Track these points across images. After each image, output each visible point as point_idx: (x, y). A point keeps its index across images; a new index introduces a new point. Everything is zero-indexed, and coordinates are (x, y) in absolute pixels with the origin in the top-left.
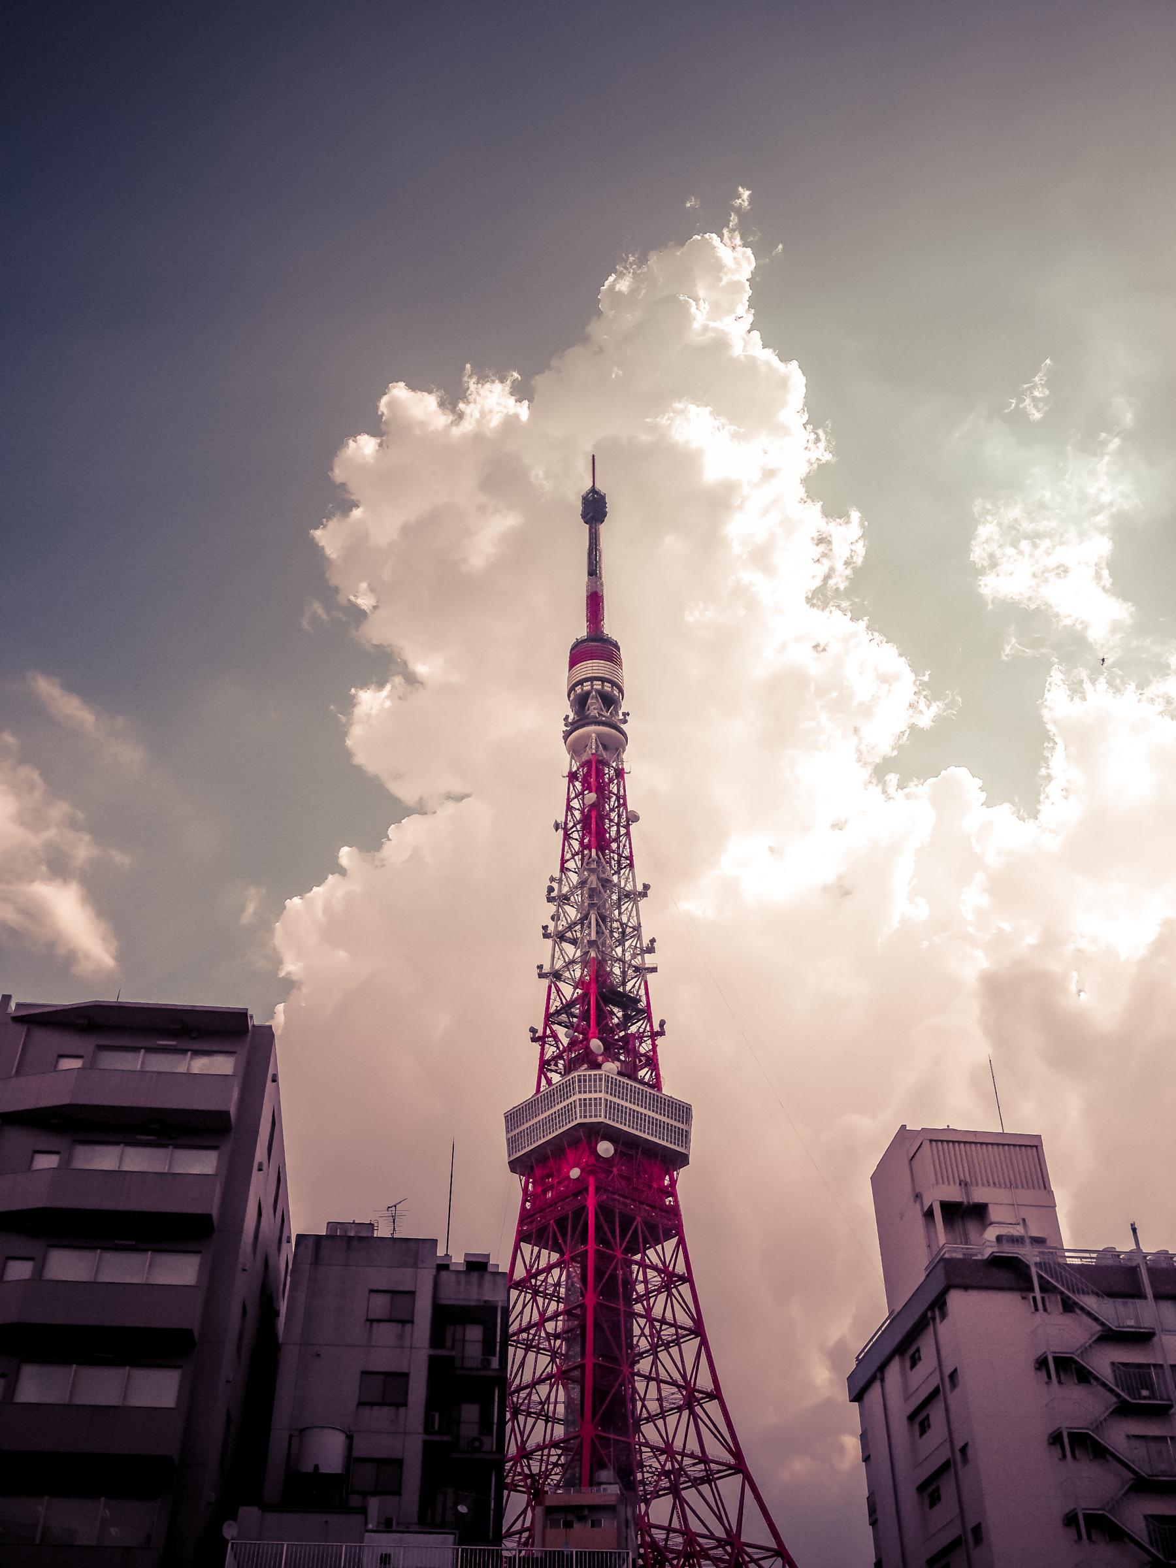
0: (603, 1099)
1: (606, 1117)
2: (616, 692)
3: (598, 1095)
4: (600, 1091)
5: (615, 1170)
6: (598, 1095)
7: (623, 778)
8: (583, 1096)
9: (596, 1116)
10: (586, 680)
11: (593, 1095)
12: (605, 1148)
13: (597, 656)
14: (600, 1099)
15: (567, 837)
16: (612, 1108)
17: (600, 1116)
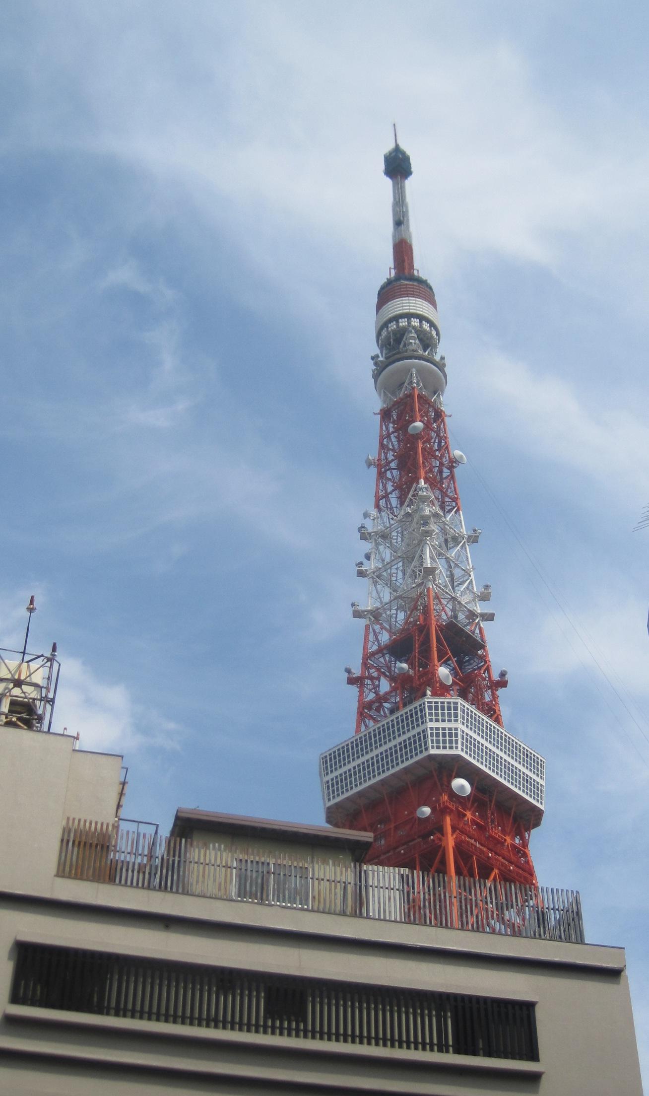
0: (459, 729)
1: (462, 750)
2: (434, 333)
3: (452, 725)
4: (456, 721)
5: (469, 815)
6: (452, 725)
7: (443, 421)
8: (434, 725)
9: (451, 748)
10: (402, 316)
11: (447, 725)
12: (461, 785)
13: (407, 294)
14: (456, 729)
15: (381, 475)
16: (469, 742)
17: (457, 748)
